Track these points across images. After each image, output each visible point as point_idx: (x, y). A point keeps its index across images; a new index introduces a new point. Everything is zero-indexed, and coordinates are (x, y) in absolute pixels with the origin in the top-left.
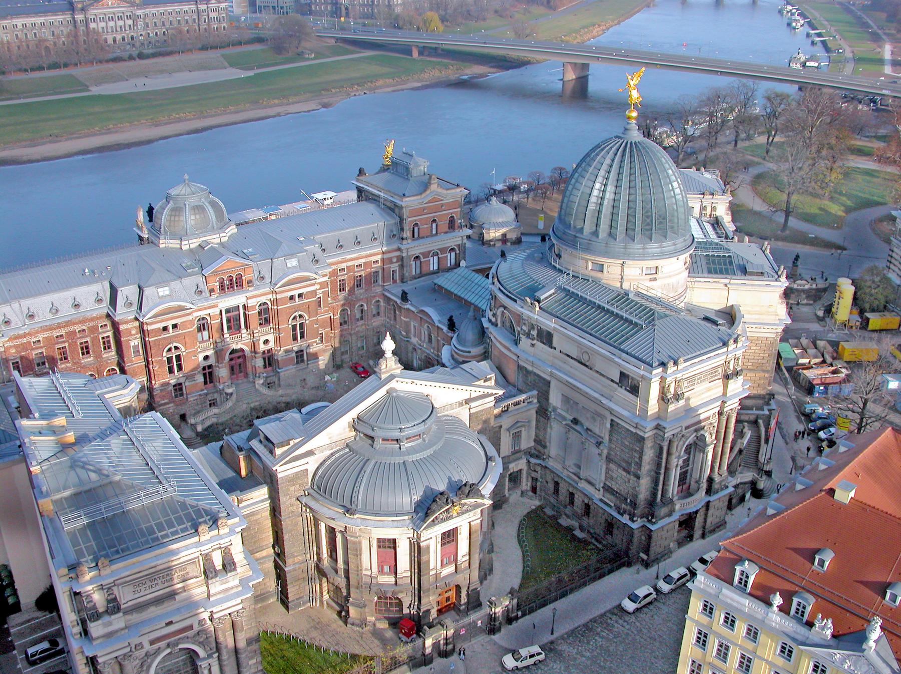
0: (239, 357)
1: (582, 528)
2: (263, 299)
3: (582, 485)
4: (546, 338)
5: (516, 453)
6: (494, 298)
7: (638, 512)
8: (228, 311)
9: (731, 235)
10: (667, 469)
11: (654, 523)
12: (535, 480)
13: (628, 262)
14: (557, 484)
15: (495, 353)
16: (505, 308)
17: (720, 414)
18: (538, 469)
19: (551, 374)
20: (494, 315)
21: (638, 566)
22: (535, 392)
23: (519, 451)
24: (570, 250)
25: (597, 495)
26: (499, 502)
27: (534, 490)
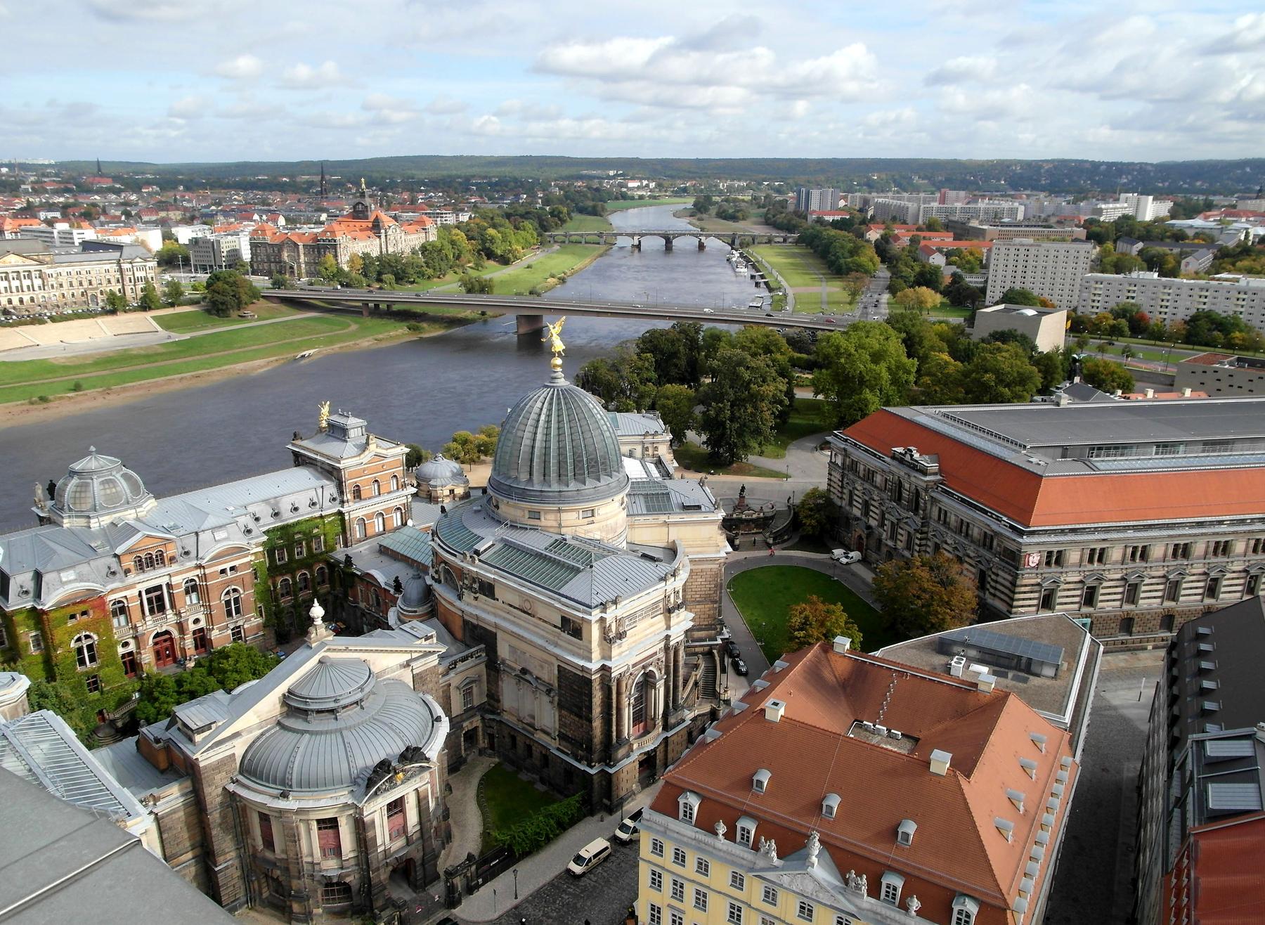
0: (165, 641)
1: (542, 781)
2: (191, 575)
3: (539, 736)
4: (487, 589)
5: (469, 712)
6: (435, 553)
7: (595, 757)
8: (148, 591)
10: (619, 710)
11: (611, 767)
12: (491, 737)
13: (564, 507)
14: (513, 738)
15: (441, 610)
16: (446, 563)
17: (667, 648)
18: (494, 724)
19: (496, 626)
20: (437, 572)
21: (603, 814)
22: (483, 646)
23: (472, 708)
24: (506, 500)
25: (553, 745)
26: (455, 764)
27: (492, 746)
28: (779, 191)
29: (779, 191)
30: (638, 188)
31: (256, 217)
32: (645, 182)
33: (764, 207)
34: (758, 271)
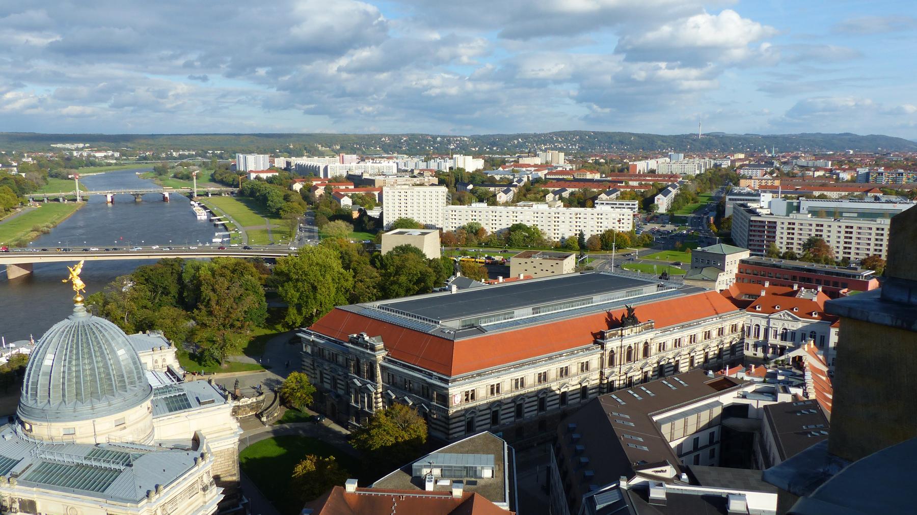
9: (181, 377)
28: (220, 157)
29: (220, 157)
30: (105, 157)
32: (110, 153)
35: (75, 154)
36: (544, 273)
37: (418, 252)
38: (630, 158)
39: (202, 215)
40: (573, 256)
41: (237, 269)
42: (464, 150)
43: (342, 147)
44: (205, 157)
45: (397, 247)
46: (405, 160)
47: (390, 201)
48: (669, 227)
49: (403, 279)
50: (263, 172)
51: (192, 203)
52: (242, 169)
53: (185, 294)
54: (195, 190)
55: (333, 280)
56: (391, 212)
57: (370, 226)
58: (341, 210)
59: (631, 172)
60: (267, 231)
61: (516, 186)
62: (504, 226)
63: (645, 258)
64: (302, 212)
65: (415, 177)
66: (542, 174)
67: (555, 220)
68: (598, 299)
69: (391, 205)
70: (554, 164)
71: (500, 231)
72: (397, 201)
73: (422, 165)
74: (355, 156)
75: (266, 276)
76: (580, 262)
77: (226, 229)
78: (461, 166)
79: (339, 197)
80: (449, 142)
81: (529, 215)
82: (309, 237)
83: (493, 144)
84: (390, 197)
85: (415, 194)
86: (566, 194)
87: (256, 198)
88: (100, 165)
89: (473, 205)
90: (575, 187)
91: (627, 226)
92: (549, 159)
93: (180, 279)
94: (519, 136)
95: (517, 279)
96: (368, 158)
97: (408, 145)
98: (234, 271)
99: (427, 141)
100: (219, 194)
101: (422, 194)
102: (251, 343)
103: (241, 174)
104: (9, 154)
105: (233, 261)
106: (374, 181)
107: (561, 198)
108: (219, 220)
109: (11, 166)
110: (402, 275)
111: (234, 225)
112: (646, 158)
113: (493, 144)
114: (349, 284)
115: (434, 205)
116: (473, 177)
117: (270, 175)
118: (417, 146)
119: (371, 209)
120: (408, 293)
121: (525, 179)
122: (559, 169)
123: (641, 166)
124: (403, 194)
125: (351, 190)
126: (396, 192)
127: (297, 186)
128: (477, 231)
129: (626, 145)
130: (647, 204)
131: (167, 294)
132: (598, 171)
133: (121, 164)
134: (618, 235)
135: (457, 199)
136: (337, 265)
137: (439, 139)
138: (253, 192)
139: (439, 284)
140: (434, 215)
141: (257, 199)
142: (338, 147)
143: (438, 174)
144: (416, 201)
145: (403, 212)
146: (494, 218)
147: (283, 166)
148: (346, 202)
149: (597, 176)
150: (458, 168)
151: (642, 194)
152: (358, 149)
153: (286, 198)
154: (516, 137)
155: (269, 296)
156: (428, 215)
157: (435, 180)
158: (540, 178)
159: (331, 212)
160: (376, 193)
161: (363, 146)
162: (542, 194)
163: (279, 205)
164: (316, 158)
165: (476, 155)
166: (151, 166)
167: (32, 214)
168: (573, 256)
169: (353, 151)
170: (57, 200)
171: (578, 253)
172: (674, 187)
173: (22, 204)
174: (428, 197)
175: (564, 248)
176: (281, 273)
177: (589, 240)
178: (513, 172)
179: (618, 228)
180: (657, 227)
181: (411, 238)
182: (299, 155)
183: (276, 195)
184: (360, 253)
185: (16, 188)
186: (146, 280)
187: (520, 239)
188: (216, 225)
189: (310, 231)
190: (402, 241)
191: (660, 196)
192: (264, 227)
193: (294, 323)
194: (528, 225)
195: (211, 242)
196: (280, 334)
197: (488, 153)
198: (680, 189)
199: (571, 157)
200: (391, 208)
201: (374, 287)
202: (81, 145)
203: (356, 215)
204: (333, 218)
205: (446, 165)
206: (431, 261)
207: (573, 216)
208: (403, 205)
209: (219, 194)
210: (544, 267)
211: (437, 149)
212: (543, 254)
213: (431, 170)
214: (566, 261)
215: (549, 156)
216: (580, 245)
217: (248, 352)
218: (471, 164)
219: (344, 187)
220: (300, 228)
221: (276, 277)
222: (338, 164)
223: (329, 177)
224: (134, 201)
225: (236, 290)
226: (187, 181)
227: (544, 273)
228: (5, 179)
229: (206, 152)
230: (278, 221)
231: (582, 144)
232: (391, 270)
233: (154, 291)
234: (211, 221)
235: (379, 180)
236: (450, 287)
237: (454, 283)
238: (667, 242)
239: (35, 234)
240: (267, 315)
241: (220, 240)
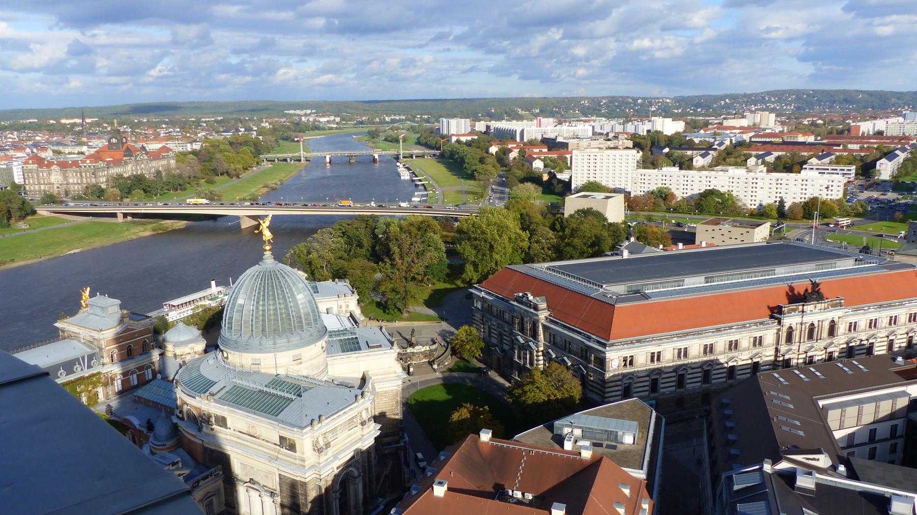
28: (428, 121)
29: (428, 121)
30: (328, 121)
31: (28, 150)
32: (332, 118)
33: (418, 133)
34: (416, 176)
35: (303, 119)
36: (733, 241)
37: (599, 216)
38: (855, 119)
39: (405, 175)
40: (767, 225)
41: (423, 227)
42: (666, 112)
43: (541, 111)
44: (414, 121)
45: (579, 211)
46: (602, 123)
47: (580, 164)
48: (891, 195)
49: (577, 241)
50: (463, 135)
51: (398, 164)
52: (445, 132)
53: (377, 248)
54: (401, 152)
55: (510, 238)
56: (579, 175)
57: (559, 188)
58: (533, 173)
59: (853, 134)
60: (461, 192)
61: (715, 149)
62: (696, 192)
63: (855, 229)
64: (494, 172)
65: (609, 140)
66: (746, 137)
67: (753, 185)
68: (781, 271)
69: (580, 168)
70: (762, 126)
71: (691, 197)
72: (586, 164)
73: (619, 128)
74: (551, 120)
75: (452, 234)
76: (776, 232)
77: (426, 189)
78: (659, 128)
79: (531, 160)
80: (651, 104)
81: (728, 180)
82: (500, 199)
83: (698, 105)
84: (580, 161)
85: (605, 157)
86: (770, 159)
87: (455, 161)
88: (324, 129)
89: (664, 169)
90: (782, 150)
91: (837, 194)
92: (757, 120)
93: (375, 236)
94: (727, 96)
95: (700, 246)
96: (565, 121)
97: (608, 107)
98: (419, 229)
99: (627, 103)
100: (423, 156)
101: (618, 157)
102: (431, 296)
103: (443, 137)
104: (251, 120)
105: (420, 219)
106: (567, 144)
107: (763, 163)
108: (420, 180)
109: (251, 130)
110: (581, 239)
111: (432, 186)
112: (875, 118)
113: (698, 105)
114: (525, 244)
115: (624, 168)
116: (671, 141)
117: (469, 138)
118: (617, 108)
119: (561, 171)
120: (582, 255)
121: (727, 142)
122: (768, 131)
123: (866, 127)
124: (592, 157)
125: (545, 153)
126: (586, 155)
127: (494, 149)
128: (666, 196)
129: (852, 103)
130: (867, 169)
131: (361, 248)
132: (813, 133)
133: (340, 128)
134: (824, 203)
135: (649, 163)
136: (513, 226)
137: (639, 101)
138: (452, 155)
139: (615, 248)
140: (623, 179)
141: (456, 161)
142: (538, 111)
143: (634, 137)
144: (605, 164)
145: (592, 175)
146: (684, 183)
147: (483, 129)
148: (538, 165)
149: (811, 139)
150: (657, 132)
151: (862, 159)
152: (557, 112)
153: (482, 161)
154: (723, 98)
155: (451, 253)
156: (617, 179)
157: (630, 144)
158: (745, 141)
159: (520, 173)
160: (568, 156)
161: (559, 109)
162: (743, 158)
163: (474, 168)
164: (514, 122)
165: (676, 117)
166: (366, 130)
167: (265, 172)
168: (767, 225)
169: (551, 114)
170: (285, 160)
171: (775, 221)
172: (903, 150)
173: (258, 163)
174: (618, 161)
175: (761, 214)
176: (460, 231)
177: (790, 208)
178: (715, 135)
179: (824, 196)
180: (875, 195)
181: (595, 201)
182: (499, 118)
183: (472, 156)
184: (544, 215)
185: (253, 150)
186: (343, 233)
187: (712, 205)
188: (417, 186)
189: (502, 192)
190: (584, 204)
191: (884, 160)
192: (459, 188)
193: (471, 280)
194: (722, 190)
195: (410, 201)
196: (459, 288)
197: (692, 115)
198: (911, 153)
199: (783, 118)
200: (579, 172)
201: (549, 249)
202: (309, 111)
203: (546, 177)
204: (523, 181)
205: (643, 128)
206: (611, 225)
207: (774, 182)
208: (592, 168)
209: (423, 156)
210: (733, 236)
211: (637, 111)
212: (734, 221)
213: (627, 133)
214: (758, 230)
215: (757, 118)
216: (780, 213)
217: (428, 303)
218: (670, 127)
219: (537, 150)
220: (492, 190)
221: (457, 235)
222: (534, 128)
223: (525, 140)
224: (348, 162)
225: (419, 247)
226: (395, 144)
227: (733, 241)
228: (246, 142)
229: (415, 117)
230: (472, 182)
231: (796, 104)
232: (567, 231)
233: (349, 243)
234: (413, 181)
235: (572, 143)
236: (622, 252)
237: (626, 248)
238: (884, 212)
239: (266, 190)
240: (448, 271)
241: (418, 199)
